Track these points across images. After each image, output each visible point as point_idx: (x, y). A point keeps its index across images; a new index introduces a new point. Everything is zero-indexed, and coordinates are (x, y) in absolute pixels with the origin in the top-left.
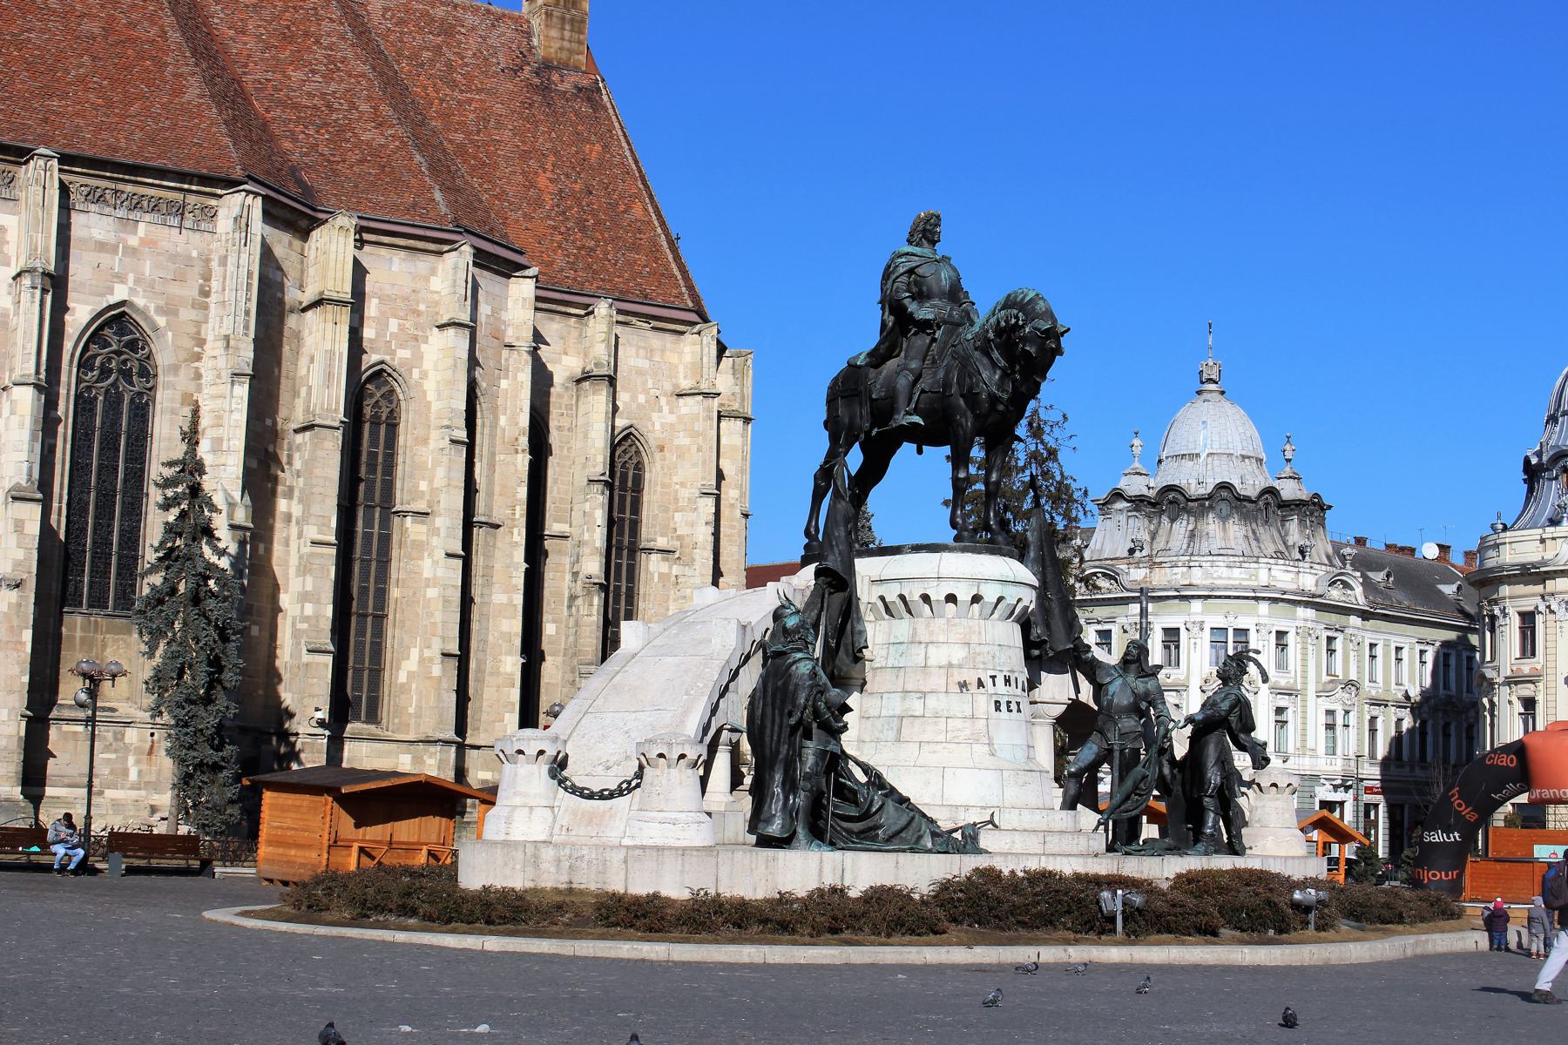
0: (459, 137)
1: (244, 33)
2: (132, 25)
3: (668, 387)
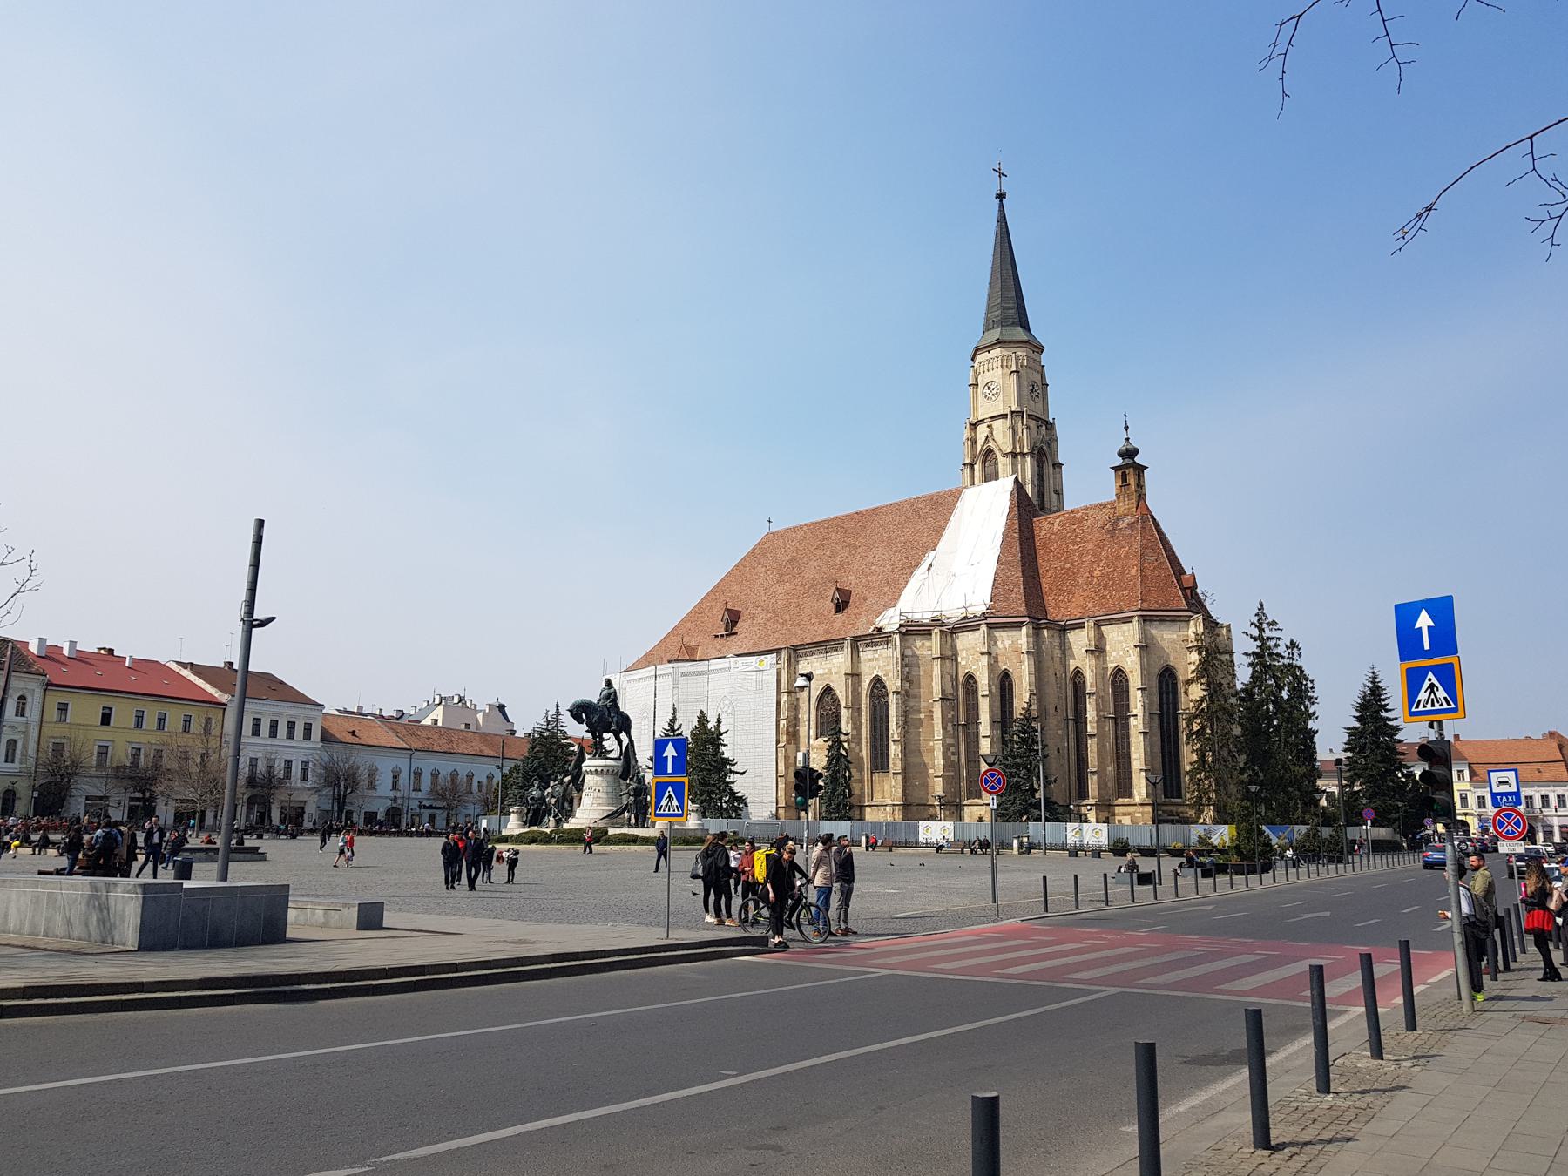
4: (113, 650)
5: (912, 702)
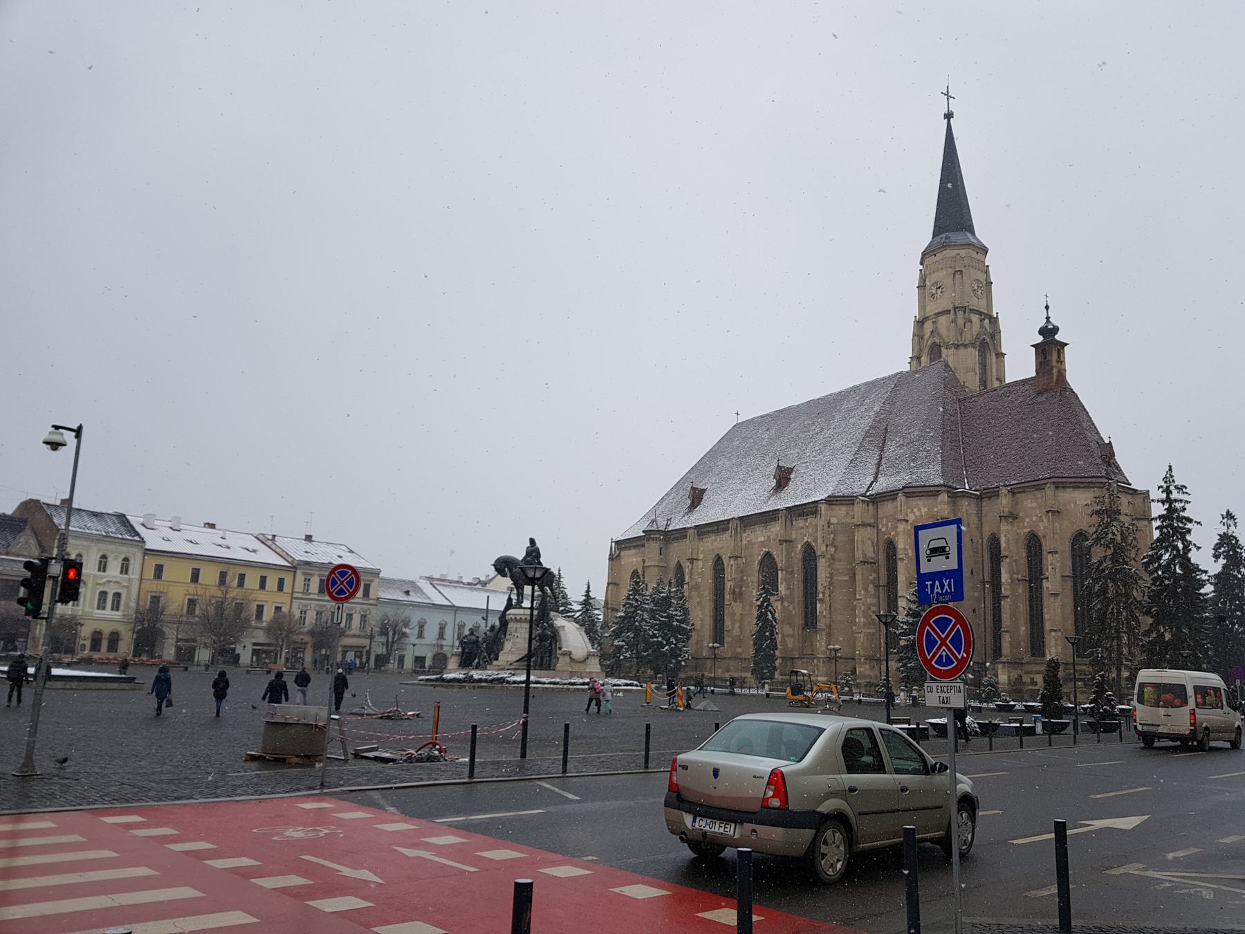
4: (311, 536)
5: (837, 565)
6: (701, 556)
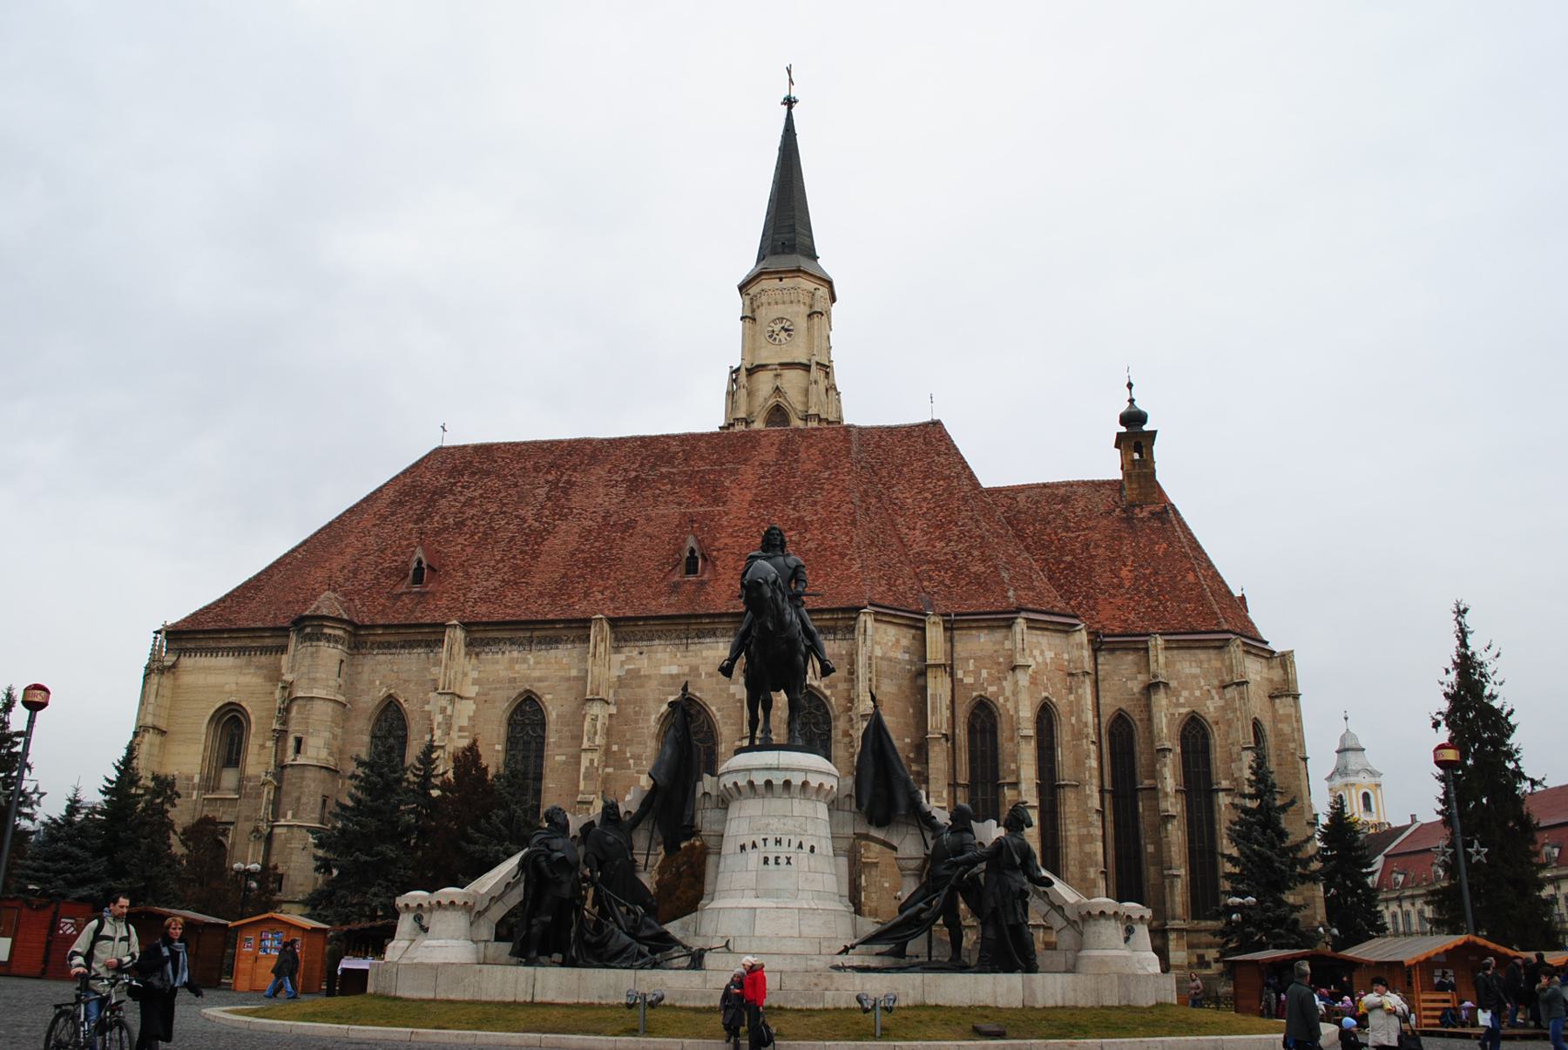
0: (1069, 558)
1: (914, 529)
2: (835, 539)
3: (1216, 683)
6: (471, 691)
